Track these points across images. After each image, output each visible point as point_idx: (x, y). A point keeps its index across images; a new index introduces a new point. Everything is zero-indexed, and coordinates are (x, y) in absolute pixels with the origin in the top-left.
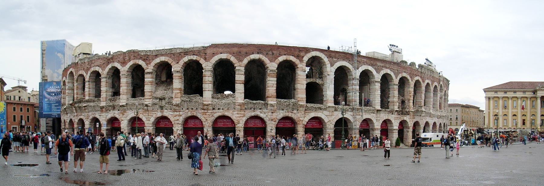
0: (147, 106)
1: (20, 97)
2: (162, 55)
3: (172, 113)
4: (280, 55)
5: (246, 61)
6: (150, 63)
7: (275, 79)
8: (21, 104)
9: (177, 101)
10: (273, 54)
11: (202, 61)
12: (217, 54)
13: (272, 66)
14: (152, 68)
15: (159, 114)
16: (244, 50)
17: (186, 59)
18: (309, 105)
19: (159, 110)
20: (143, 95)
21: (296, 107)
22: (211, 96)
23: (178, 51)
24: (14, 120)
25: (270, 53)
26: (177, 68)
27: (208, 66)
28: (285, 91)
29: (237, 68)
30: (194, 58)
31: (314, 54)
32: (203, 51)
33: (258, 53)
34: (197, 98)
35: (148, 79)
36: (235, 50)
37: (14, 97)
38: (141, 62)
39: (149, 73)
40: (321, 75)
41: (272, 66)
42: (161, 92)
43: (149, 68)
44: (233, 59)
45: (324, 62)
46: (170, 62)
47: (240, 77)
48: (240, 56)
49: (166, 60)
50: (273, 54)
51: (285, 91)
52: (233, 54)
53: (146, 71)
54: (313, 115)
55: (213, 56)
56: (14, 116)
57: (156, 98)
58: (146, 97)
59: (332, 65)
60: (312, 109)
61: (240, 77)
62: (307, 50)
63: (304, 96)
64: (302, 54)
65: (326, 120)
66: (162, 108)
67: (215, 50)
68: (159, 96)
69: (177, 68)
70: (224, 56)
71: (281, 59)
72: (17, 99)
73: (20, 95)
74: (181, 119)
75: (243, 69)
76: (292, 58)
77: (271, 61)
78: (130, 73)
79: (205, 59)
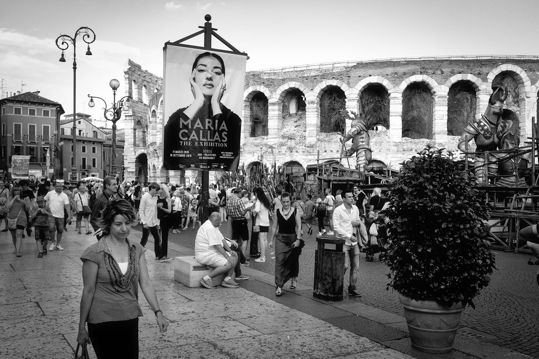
0: (271, 147)
2: (291, 80)
3: (305, 157)
4: (453, 73)
5: (404, 85)
6: (275, 91)
7: (446, 108)
8: (84, 142)
9: (311, 140)
10: (442, 72)
11: (344, 87)
12: (365, 77)
14: (278, 97)
15: (288, 159)
17: (324, 85)
19: (288, 153)
20: (265, 132)
23: (313, 74)
25: (439, 72)
26: (311, 96)
29: (392, 95)
30: (334, 83)
31: (504, 67)
32: (346, 73)
33: (421, 73)
35: (274, 112)
38: (262, 89)
39: (273, 104)
42: (290, 128)
43: (274, 97)
44: (385, 83)
45: (521, 79)
46: (301, 89)
47: (396, 107)
48: (397, 78)
49: (297, 87)
50: (442, 72)
53: (270, 101)
55: (360, 80)
57: (283, 137)
58: (269, 136)
61: (396, 107)
62: (493, 63)
64: (484, 70)
66: (291, 149)
68: (288, 134)
69: (311, 96)
70: (374, 80)
71: (454, 79)
75: (400, 96)
76: (470, 77)
77: (440, 83)
78: (248, 104)
79: (348, 84)
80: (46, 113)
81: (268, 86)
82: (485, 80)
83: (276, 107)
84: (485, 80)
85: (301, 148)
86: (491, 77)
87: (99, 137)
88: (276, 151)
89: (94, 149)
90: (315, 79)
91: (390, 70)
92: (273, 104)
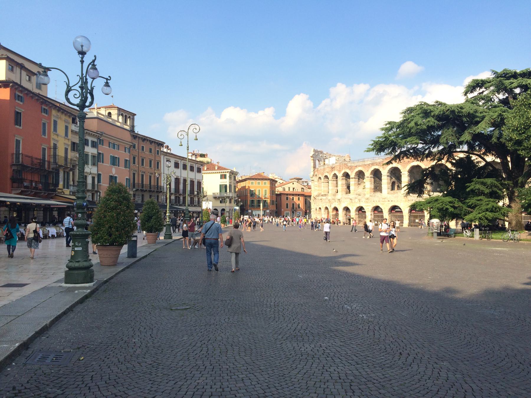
1: (294, 188)
5: (408, 167)
9: (367, 196)
17: (373, 168)
22: (387, 193)
24: (287, 207)
30: (377, 167)
34: (378, 194)
37: (289, 188)
39: (352, 178)
42: (360, 189)
43: (352, 175)
56: (287, 204)
68: (358, 193)
69: (368, 174)
72: (291, 190)
73: (294, 186)
80: (265, 183)
81: (350, 169)
83: (354, 180)
85: (363, 200)
87: (305, 191)
88: (353, 201)
89: (299, 198)
92: (352, 178)
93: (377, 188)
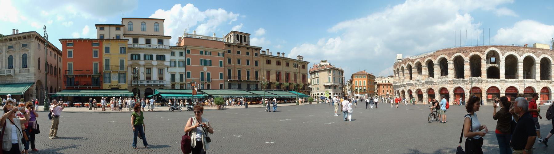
4: (471, 52)
5: (453, 58)
11: (433, 60)
13: (467, 59)
15: (417, 88)
16: (451, 52)
17: (426, 60)
18: (489, 80)
21: (480, 81)
26: (424, 64)
27: (435, 62)
28: (476, 72)
30: (430, 58)
31: (491, 49)
36: (448, 52)
40: (497, 61)
41: (467, 59)
44: (446, 57)
47: (451, 66)
48: (450, 55)
51: (476, 72)
52: (446, 54)
54: (491, 85)
59: (503, 55)
60: (490, 82)
61: (451, 66)
62: (487, 47)
63: (486, 74)
64: (483, 50)
65: (500, 88)
67: (438, 53)
70: (443, 56)
71: (471, 54)
74: (425, 90)
75: (452, 62)
76: (477, 53)
77: (466, 56)
82: (483, 54)
84: (483, 54)
86: (486, 52)
90: (425, 58)
91: (448, 52)
93: (431, 74)
